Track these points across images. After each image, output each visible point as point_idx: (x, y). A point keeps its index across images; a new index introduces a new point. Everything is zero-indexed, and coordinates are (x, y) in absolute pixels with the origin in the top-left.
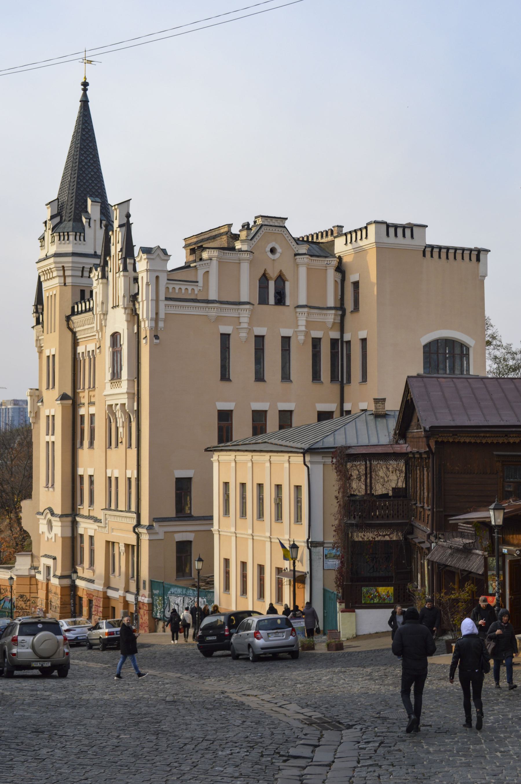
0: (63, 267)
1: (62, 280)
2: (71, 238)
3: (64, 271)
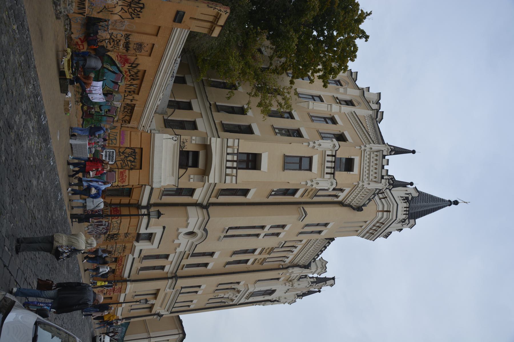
0: (390, 211)
1: (381, 209)
2: (404, 217)
3: (387, 211)
